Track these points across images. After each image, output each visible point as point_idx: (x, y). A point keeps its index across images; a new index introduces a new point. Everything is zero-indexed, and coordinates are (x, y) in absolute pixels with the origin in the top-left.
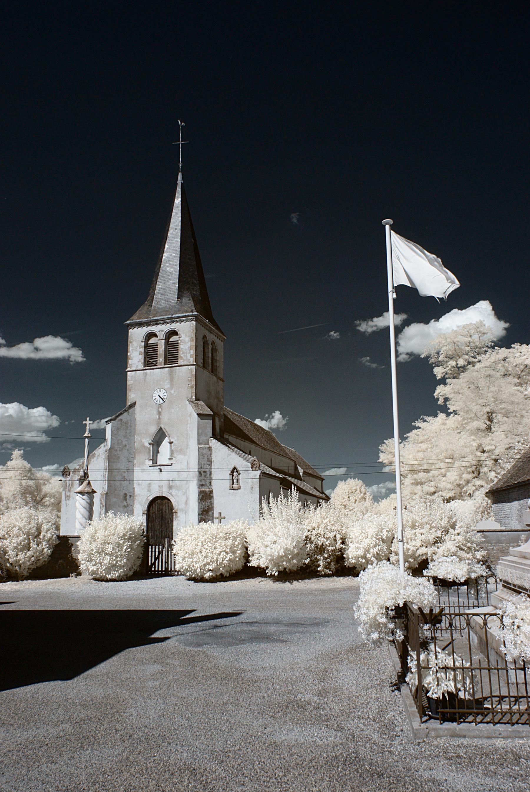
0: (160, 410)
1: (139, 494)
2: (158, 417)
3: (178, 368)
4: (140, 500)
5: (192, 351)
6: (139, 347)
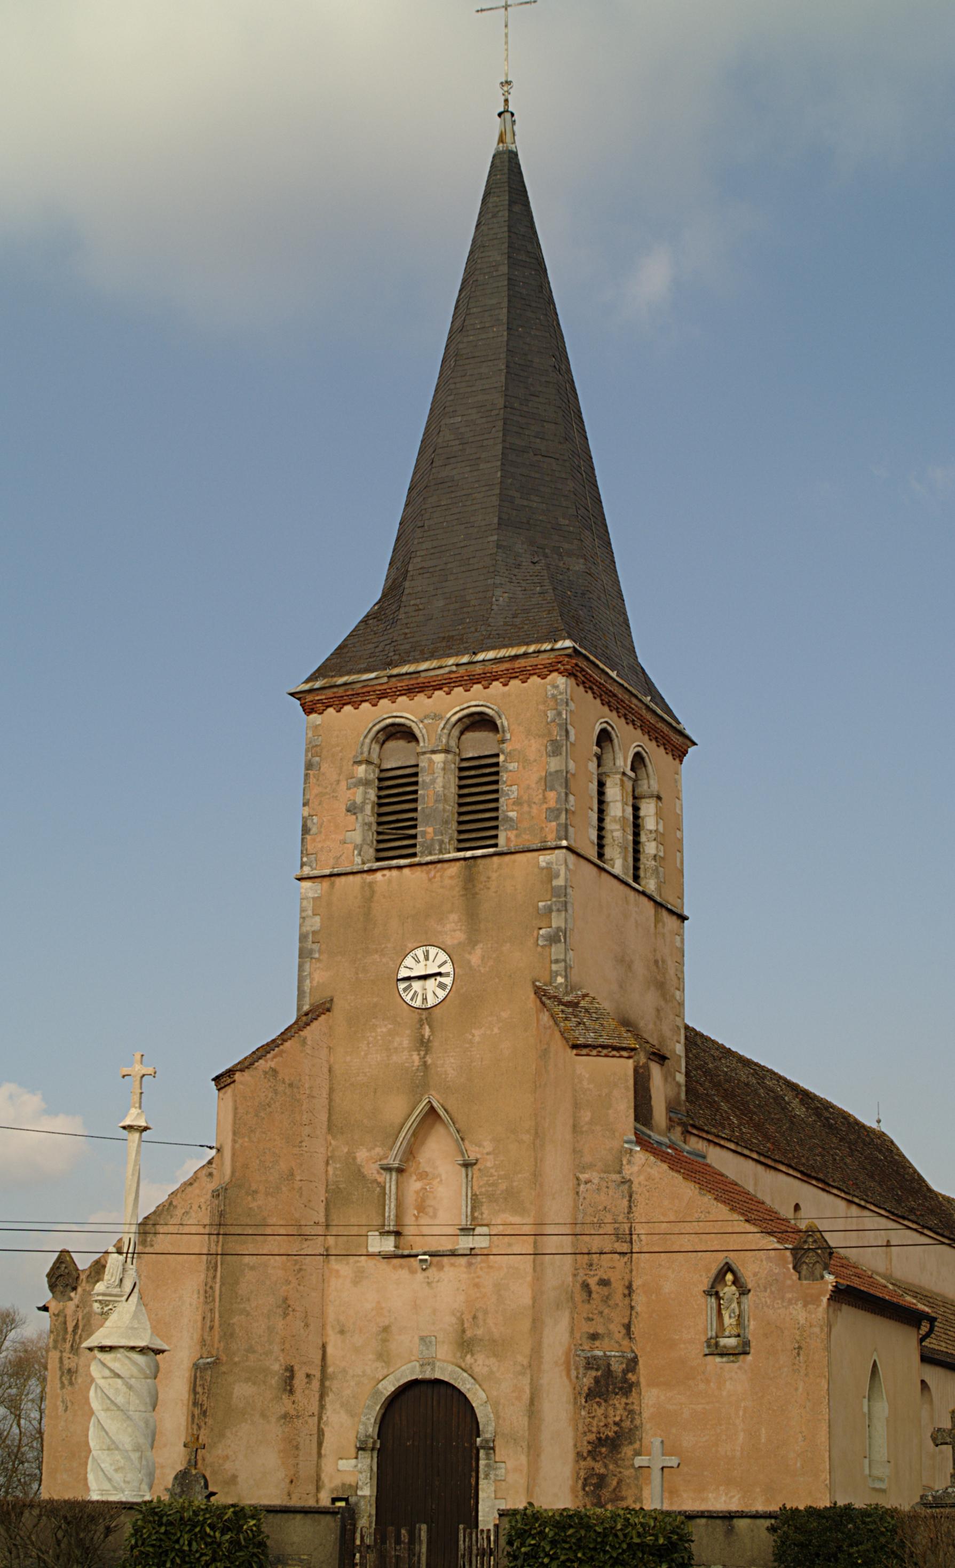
0: (427, 1031)
1: (344, 1371)
2: (416, 1058)
3: (495, 859)
6: (343, 785)
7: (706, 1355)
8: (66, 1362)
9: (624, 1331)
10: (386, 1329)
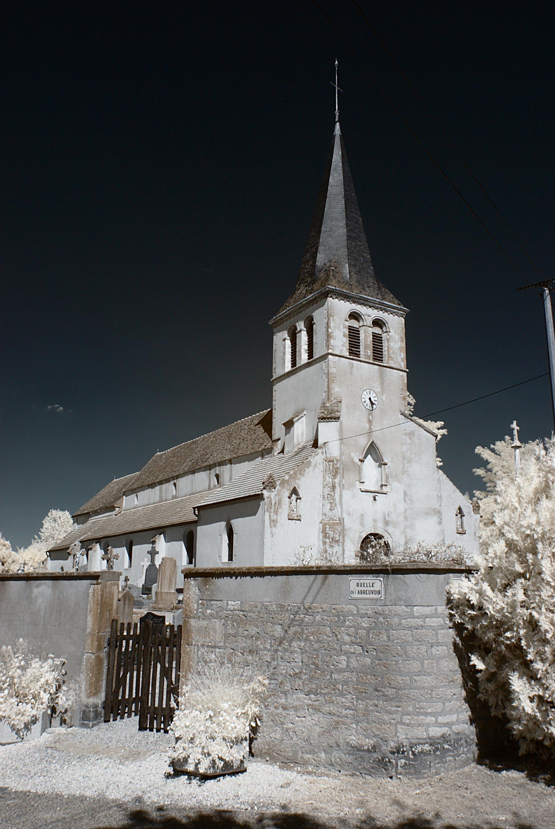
0: (371, 418)
1: (350, 528)
4: (351, 536)
5: (402, 354)
8: (272, 517)
10: (362, 515)
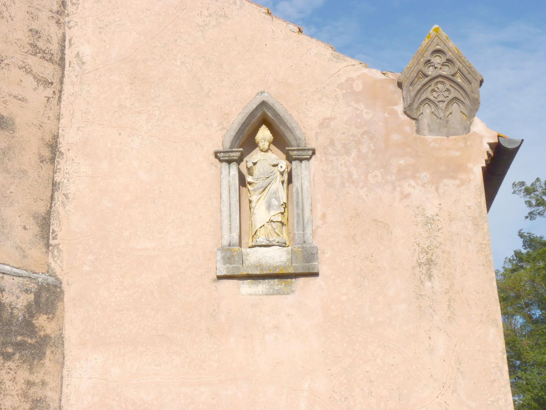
7: (220, 278)
9: (34, 228)
